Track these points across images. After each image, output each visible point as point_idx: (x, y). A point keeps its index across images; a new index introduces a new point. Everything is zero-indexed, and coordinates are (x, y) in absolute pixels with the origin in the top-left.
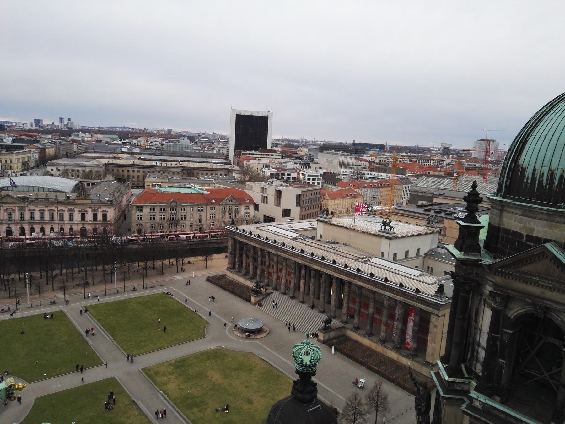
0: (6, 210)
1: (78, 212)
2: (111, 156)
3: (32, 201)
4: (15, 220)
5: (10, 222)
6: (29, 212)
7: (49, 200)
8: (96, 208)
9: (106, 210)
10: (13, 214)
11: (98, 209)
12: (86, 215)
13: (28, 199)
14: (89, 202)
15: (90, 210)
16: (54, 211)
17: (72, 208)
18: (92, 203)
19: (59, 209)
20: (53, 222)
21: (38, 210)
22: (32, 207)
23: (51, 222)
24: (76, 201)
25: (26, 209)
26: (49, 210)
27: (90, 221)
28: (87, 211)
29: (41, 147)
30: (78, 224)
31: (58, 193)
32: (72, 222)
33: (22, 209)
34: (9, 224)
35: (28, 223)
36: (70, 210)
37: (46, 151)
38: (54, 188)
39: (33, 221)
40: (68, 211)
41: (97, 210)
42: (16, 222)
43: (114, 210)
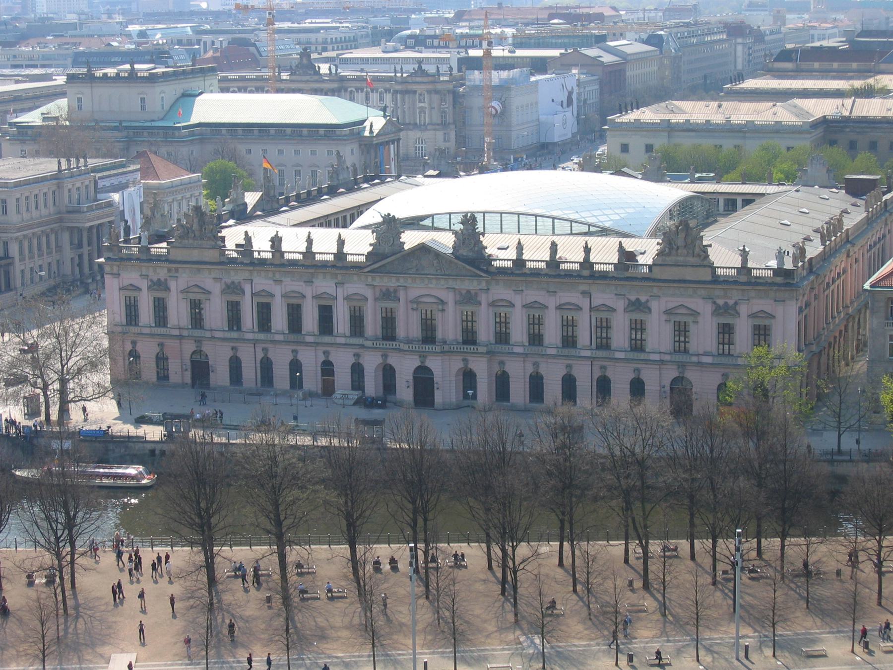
0: (416, 301)
1: (664, 317)
2: (858, 84)
3: (502, 271)
4: (445, 342)
5: (428, 347)
6: (491, 311)
7: (562, 266)
8: (731, 302)
9: (768, 309)
10: (438, 316)
11: (736, 303)
12: (692, 328)
13: (489, 260)
14: (705, 275)
15: (705, 309)
16: (579, 309)
17: (643, 299)
18: (716, 280)
19: (596, 302)
20: (572, 352)
21: (523, 306)
22: (500, 292)
23: (566, 351)
24: (658, 273)
25: (483, 298)
26: (559, 307)
27: (706, 354)
28: (695, 314)
29: (607, 58)
30: (662, 362)
31: (592, 241)
32: (642, 356)
33: (469, 298)
34: (423, 356)
35: (488, 353)
36: (637, 306)
37: (629, 73)
38: (591, 220)
39: (505, 348)
40: (625, 310)
41: (729, 310)
42: (446, 348)
43: (800, 310)
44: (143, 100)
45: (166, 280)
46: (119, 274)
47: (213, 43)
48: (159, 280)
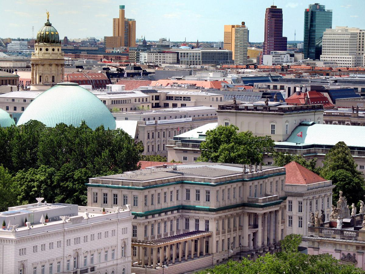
44: (273, 127)
45: (354, 255)
46: (319, 248)
47: (295, 88)
48: (349, 254)
